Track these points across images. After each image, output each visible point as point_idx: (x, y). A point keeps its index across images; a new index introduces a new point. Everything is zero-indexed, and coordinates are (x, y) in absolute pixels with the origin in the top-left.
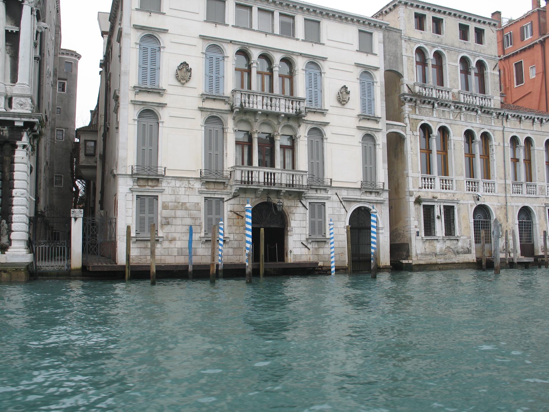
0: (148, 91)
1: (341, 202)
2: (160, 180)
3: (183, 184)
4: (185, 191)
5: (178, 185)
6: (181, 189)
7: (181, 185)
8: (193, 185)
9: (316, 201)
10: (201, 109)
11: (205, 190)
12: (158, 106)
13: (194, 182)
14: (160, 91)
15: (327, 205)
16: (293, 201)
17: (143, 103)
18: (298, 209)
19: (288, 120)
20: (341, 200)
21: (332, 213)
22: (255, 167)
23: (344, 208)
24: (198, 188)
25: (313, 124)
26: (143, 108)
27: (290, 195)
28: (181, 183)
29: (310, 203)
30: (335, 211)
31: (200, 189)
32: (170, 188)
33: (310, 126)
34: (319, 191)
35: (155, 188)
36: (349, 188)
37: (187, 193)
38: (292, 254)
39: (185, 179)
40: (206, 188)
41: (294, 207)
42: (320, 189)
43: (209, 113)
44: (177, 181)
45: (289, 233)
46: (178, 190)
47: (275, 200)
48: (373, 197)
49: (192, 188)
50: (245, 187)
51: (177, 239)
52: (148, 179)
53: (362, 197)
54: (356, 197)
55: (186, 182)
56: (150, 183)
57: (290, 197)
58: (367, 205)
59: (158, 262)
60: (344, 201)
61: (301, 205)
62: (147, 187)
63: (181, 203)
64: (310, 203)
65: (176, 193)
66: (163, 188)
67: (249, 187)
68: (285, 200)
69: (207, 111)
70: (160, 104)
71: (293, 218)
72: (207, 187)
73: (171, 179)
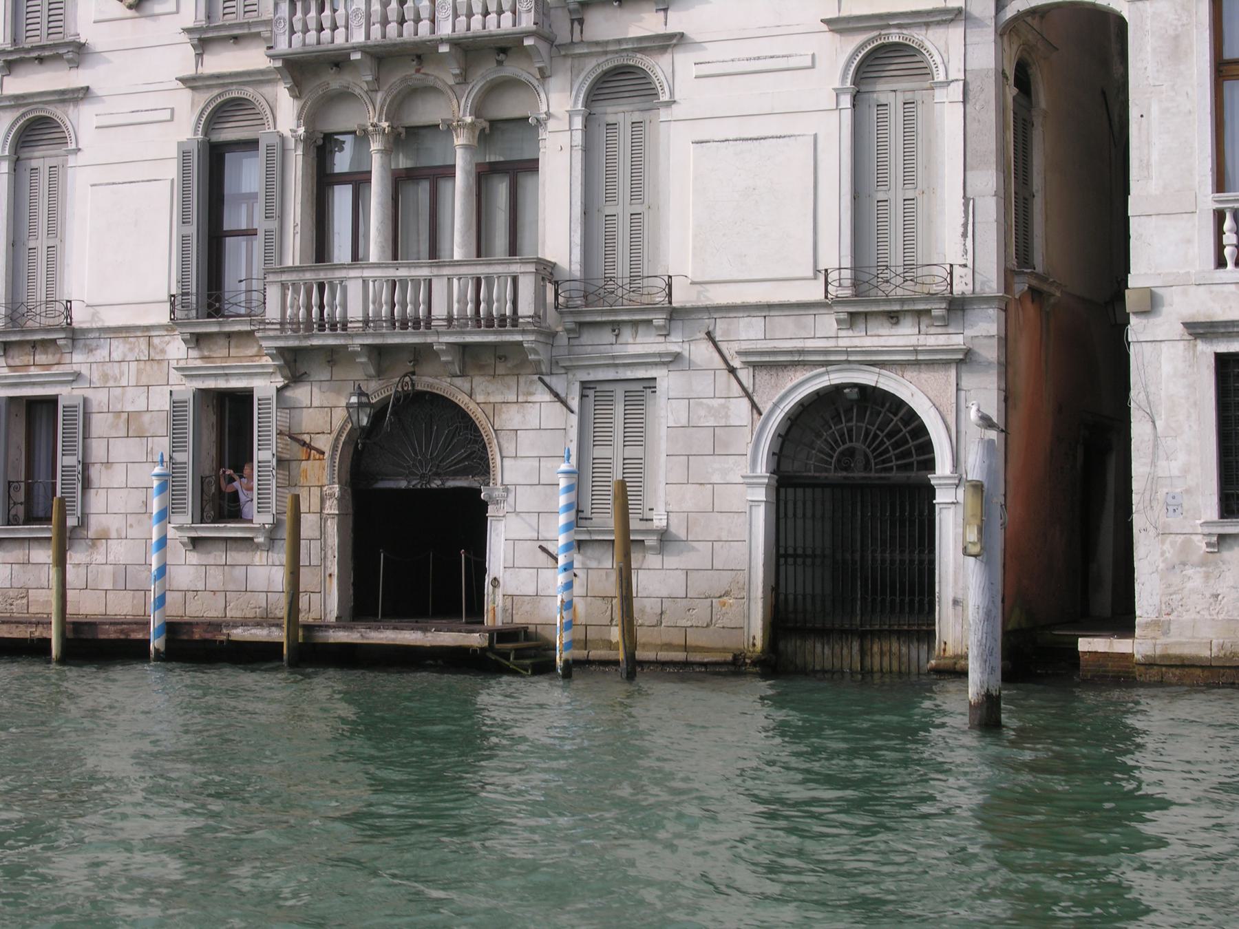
0: (43, 57)
1: (732, 371)
2: (59, 342)
3: (131, 350)
4: (139, 372)
5: (116, 356)
6: (125, 365)
7: (125, 355)
8: (163, 351)
9: (610, 374)
10: (191, 83)
11: (199, 363)
12: (63, 101)
13: (167, 338)
14: (61, 51)
15: (662, 385)
16: (512, 381)
17: (19, 100)
18: (532, 411)
19: (500, 63)
20: (736, 363)
21: (684, 422)
22: (342, 267)
23: (748, 395)
24: (178, 360)
25: (606, 53)
26: (23, 115)
27: (502, 358)
28: (128, 346)
29: (585, 385)
30: (702, 412)
31: (182, 364)
32: (94, 366)
33: (593, 67)
34: (627, 335)
35: (55, 370)
36: (770, 307)
37: (144, 381)
38: (500, 592)
39: (139, 334)
40: (202, 358)
41: (514, 408)
42: (635, 324)
43: (216, 92)
44: (115, 343)
45: (491, 510)
46: (117, 372)
47: (431, 381)
48: (903, 337)
49: (159, 361)
50: (331, 342)
51: (114, 534)
52: (34, 345)
53: (843, 343)
54: (798, 344)
55: (143, 343)
56: (41, 358)
57: (501, 369)
58: (867, 378)
59: (174, 610)
60: (747, 364)
61: (548, 397)
62: (33, 371)
63: (125, 416)
64: (585, 385)
65: (111, 383)
66: (76, 368)
67: (316, 342)
68: (477, 380)
69: (209, 87)
70: (63, 92)
71: (509, 449)
72: (206, 354)
73: (97, 335)
